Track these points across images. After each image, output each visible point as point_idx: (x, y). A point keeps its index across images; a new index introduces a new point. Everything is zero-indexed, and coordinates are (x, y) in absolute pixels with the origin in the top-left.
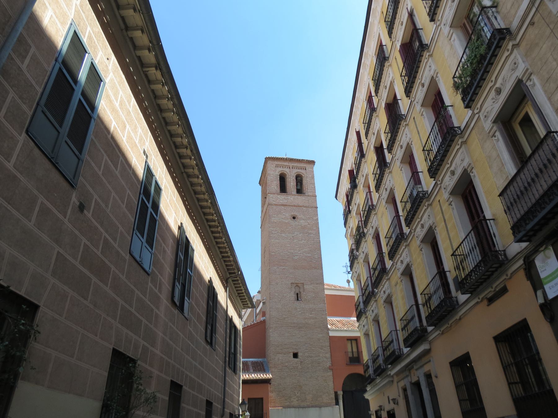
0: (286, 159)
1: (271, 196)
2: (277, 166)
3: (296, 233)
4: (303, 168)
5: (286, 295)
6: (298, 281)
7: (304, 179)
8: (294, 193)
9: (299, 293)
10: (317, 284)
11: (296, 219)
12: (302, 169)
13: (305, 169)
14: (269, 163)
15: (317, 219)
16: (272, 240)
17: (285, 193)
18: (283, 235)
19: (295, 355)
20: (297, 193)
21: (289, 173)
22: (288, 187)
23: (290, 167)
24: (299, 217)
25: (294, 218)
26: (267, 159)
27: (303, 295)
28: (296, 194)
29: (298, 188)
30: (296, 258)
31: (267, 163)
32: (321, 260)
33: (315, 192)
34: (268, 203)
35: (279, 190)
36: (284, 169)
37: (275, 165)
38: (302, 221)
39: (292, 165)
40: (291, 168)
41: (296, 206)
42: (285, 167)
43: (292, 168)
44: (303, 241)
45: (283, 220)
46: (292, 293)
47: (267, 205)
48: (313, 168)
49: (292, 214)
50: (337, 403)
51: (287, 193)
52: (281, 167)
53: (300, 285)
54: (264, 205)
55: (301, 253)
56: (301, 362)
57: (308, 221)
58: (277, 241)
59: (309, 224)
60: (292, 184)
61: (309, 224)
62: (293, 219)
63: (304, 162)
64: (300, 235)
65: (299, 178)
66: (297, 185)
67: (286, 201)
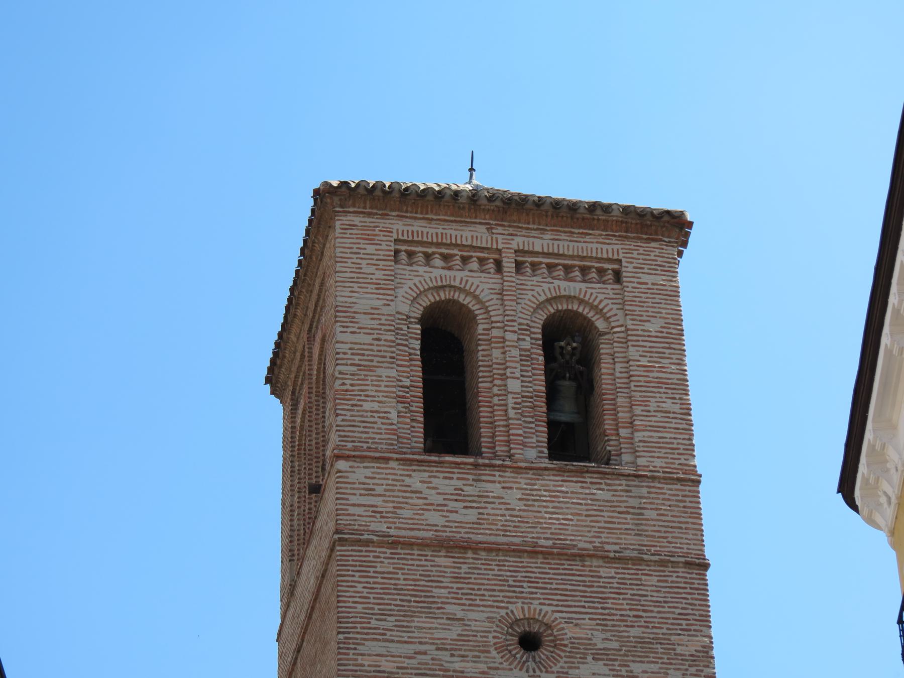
0: (474, 196)
1: (361, 473)
4: (601, 272)
7: (604, 349)
8: (532, 454)
11: (542, 654)
13: (618, 276)
17: (465, 452)
20: (552, 457)
21: (493, 303)
22: (484, 413)
23: (498, 264)
24: (570, 632)
28: (546, 463)
29: (564, 418)
31: (331, 227)
33: (690, 449)
34: (332, 526)
35: (420, 428)
36: (457, 277)
37: (387, 247)
39: (518, 242)
40: (509, 265)
41: (547, 554)
42: (465, 260)
43: (519, 266)
45: (445, 656)
47: (326, 544)
48: (671, 271)
49: (517, 610)
51: (479, 454)
52: (438, 262)
54: (306, 542)
60: (514, 385)
62: (520, 653)
63: (606, 226)
65: (568, 345)
66: (552, 395)
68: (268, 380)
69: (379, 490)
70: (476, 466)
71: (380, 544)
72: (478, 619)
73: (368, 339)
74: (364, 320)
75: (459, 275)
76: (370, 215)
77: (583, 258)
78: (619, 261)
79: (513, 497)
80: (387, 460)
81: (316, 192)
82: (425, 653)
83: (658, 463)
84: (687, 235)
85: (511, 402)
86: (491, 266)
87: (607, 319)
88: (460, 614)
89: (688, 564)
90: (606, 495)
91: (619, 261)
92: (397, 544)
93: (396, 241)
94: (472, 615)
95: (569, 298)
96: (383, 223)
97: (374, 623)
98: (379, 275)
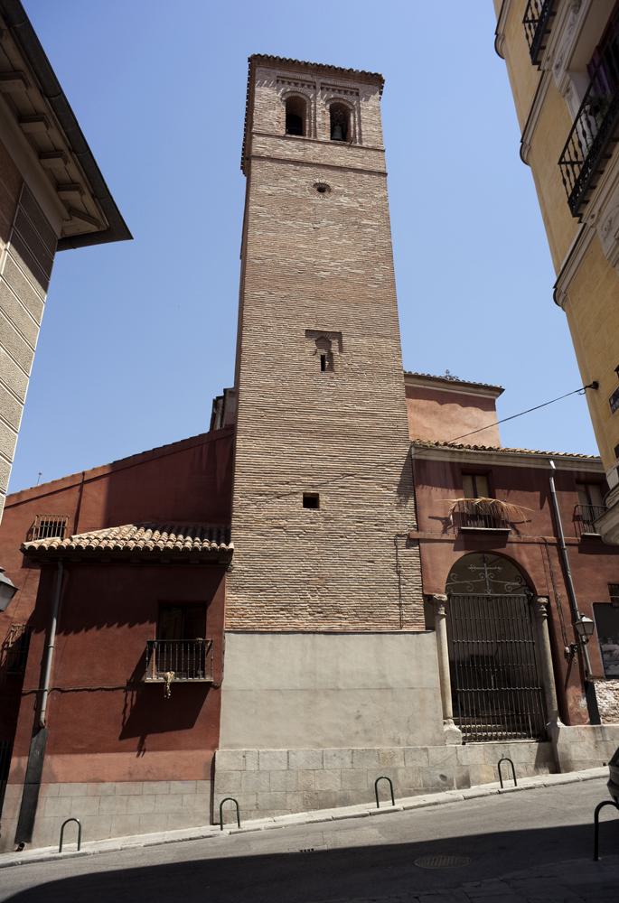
1: (261, 139)
3: (325, 222)
10: (382, 336)
11: (326, 194)
13: (357, 94)
15: (385, 198)
18: (289, 223)
19: (311, 501)
23: (315, 87)
25: (322, 189)
26: (257, 62)
36: (300, 89)
38: (342, 199)
39: (322, 80)
40: (318, 86)
49: (317, 181)
50: (431, 626)
51: (304, 135)
55: (337, 266)
56: (328, 519)
57: (360, 200)
58: (272, 235)
60: (319, 119)
62: (317, 193)
72: (302, 182)
79: (317, 150)
81: (250, 60)
84: (382, 87)
88: (295, 179)
95: (340, 99)
96: (273, 71)
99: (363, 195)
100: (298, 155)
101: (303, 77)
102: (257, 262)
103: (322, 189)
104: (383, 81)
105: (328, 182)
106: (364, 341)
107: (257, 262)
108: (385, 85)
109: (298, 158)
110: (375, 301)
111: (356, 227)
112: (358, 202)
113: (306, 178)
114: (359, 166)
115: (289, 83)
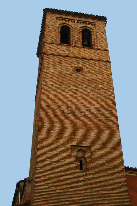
1: (49, 45)
2: (59, 19)
5: (63, 161)
6: (82, 143)
9: (83, 160)
10: (112, 149)
12: (91, 24)
13: (95, 25)
14: (48, 16)
15: (110, 74)
16: (47, 92)
17: (68, 44)
18: (63, 87)
23: (74, 22)
25: (78, 70)
27: (90, 161)
30: (80, 114)
31: (46, 15)
32: (117, 120)
36: (67, 23)
38: (88, 75)
40: (76, 21)
41: (81, 58)
43: (78, 22)
44: (91, 96)
46: (73, 160)
52: (64, 20)
53: (84, 149)
55: (87, 110)
57: (98, 75)
59: (98, 78)
60: (77, 36)
61: (98, 78)
64: (87, 89)
67: (68, 52)
68: (37, 54)
69: (52, 48)
70: (70, 46)
71: (51, 55)
72: (69, 66)
73: (51, 29)
74: (51, 26)
75: (67, 22)
76: (52, 13)
77: (89, 22)
78: (95, 23)
79: (76, 50)
80: (54, 44)
81: (44, 10)
82: (59, 70)
83: (102, 48)
84: (106, 22)
85: (76, 38)
86: (73, 22)
87: (93, 30)
88: (66, 65)
89: (107, 62)
90: (93, 52)
91: (95, 23)
92: (54, 55)
93: (57, 17)
94: (68, 66)
96: (56, 15)
97: (50, 65)
98: (54, 21)
99: (99, 72)
100: (67, 53)
101: (69, 17)
102: (45, 107)
103: (78, 70)
104: (107, 19)
105: (82, 66)
106: (103, 151)
107: (45, 107)
108: (107, 21)
109: (66, 55)
110: (108, 129)
111: (96, 89)
112: (97, 76)
113: (70, 65)
114: (97, 58)
115: (62, 20)
